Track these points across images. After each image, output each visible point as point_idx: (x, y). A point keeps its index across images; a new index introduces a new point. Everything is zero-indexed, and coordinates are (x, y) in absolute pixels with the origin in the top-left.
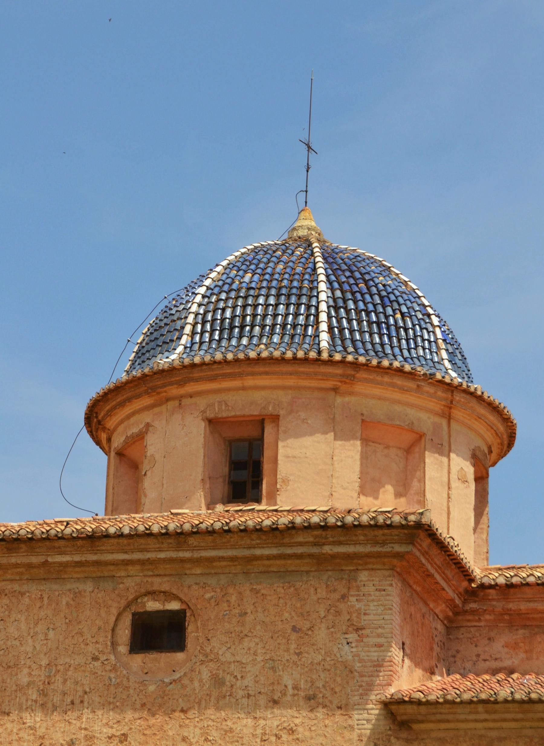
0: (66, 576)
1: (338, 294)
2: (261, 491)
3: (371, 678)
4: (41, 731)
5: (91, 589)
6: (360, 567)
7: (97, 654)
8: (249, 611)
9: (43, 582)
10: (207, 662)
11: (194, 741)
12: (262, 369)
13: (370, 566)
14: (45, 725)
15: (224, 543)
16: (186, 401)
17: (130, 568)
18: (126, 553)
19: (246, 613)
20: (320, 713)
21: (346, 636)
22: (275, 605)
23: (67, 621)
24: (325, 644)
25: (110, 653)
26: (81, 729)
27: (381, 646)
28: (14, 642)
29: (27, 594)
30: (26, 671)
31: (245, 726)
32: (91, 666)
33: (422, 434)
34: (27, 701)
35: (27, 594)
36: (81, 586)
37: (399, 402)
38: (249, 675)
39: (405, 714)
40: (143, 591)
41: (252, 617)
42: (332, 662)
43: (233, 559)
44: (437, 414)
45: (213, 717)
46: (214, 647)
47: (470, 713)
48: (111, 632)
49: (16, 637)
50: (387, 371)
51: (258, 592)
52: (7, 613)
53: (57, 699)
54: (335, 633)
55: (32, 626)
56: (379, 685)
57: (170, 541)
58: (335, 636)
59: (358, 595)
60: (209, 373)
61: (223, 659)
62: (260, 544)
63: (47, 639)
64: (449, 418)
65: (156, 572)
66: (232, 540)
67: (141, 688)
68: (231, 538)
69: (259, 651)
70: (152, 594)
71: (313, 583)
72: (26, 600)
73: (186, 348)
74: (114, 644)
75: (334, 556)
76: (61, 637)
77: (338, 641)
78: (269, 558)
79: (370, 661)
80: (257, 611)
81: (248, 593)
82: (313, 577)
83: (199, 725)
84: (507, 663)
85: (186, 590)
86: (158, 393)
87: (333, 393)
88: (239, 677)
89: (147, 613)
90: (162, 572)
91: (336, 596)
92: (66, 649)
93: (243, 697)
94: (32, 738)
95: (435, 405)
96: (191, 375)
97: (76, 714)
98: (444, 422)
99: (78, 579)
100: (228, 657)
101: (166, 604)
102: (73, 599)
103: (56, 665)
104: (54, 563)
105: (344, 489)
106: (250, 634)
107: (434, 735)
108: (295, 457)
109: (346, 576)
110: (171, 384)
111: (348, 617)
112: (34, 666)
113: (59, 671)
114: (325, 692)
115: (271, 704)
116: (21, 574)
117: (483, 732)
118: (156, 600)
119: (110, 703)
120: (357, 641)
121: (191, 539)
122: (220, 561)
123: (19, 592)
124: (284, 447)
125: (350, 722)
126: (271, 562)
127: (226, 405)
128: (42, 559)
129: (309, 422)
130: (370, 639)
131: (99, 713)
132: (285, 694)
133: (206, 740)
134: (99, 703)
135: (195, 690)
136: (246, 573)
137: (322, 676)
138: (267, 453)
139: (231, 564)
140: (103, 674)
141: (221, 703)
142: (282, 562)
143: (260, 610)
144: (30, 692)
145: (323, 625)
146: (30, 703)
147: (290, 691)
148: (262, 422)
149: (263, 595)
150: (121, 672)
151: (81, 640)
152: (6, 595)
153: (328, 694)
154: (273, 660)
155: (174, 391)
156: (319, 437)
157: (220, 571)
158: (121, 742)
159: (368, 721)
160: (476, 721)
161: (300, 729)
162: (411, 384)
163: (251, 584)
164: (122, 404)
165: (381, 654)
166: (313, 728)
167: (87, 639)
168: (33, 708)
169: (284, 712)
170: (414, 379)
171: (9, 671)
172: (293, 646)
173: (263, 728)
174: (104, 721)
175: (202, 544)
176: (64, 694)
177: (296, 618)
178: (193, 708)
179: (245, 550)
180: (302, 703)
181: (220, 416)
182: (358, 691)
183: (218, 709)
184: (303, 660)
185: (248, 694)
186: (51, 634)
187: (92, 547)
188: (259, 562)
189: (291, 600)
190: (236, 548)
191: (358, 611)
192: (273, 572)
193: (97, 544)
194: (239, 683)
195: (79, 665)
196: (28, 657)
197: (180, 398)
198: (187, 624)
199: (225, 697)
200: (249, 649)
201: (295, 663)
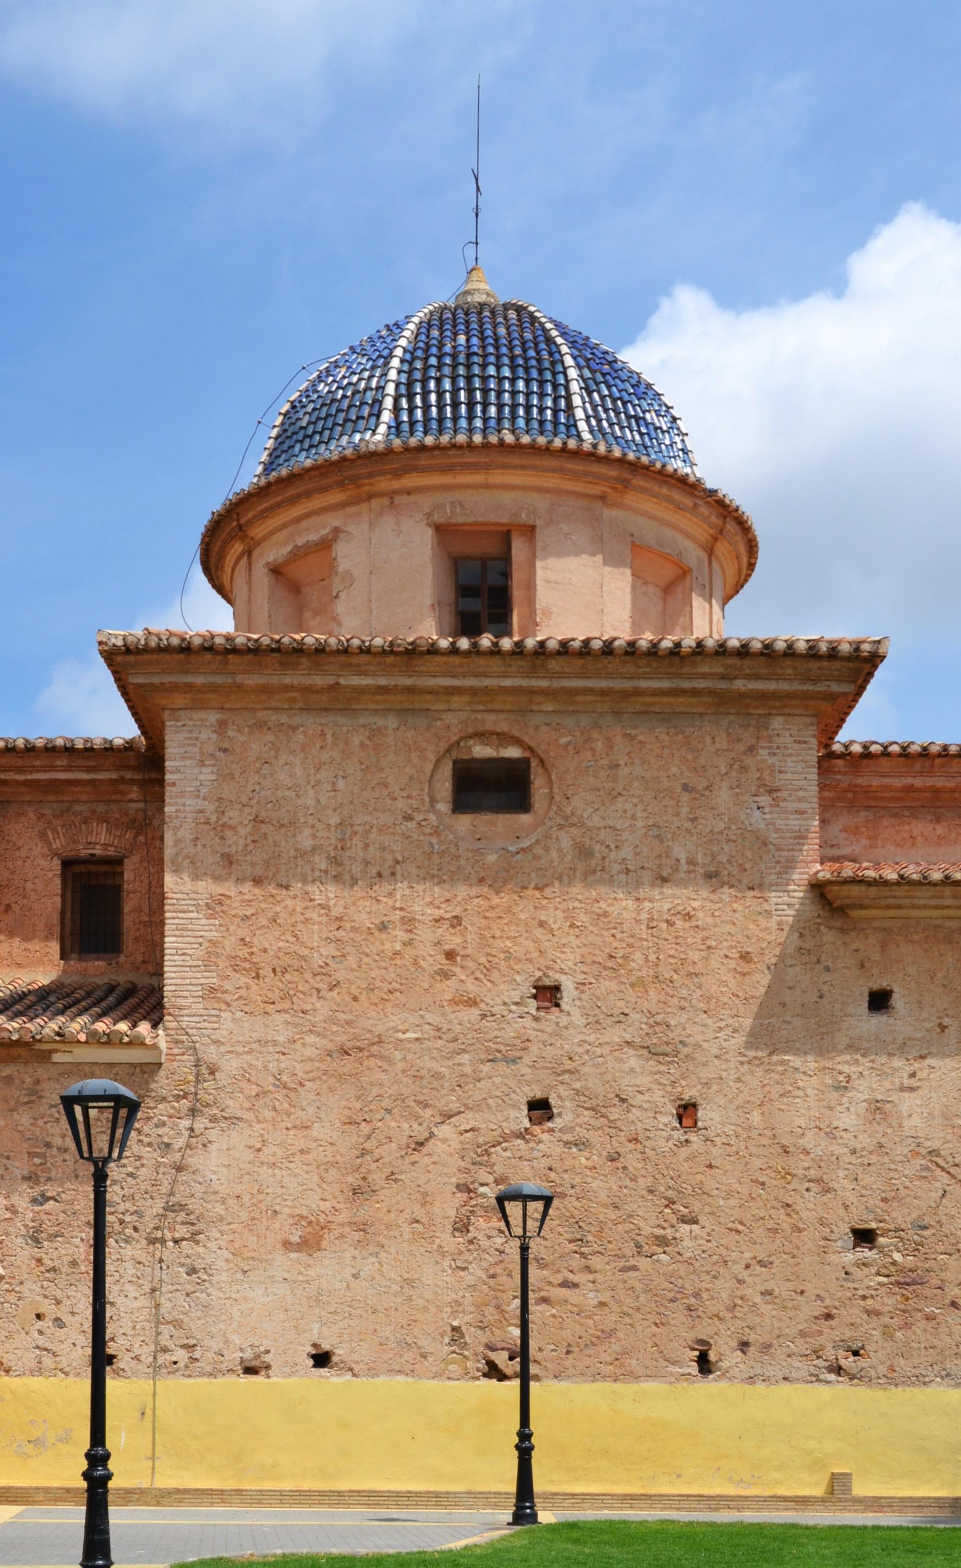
0: (358, 707)
2: (511, 625)
3: (791, 853)
4: (337, 911)
5: (395, 725)
6: (774, 712)
7: (409, 812)
8: (622, 762)
9: (324, 714)
10: (568, 826)
11: (555, 926)
12: (518, 461)
13: (787, 711)
14: (342, 902)
15: (599, 669)
16: (401, 500)
17: (455, 698)
18: (455, 677)
19: (618, 766)
20: (726, 893)
21: (757, 799)
22: (657, 756)
23: (363, 767)
24: (729, 809)
25: (429, 812)
26: (395, 908)
27: (803, 812)
28: (287, 793)
29: (302, 729)
30: (307, 832)
31: (625, 909)
32: (403, 827)
33: (686, 568)
34: (313, 870)
35: (302, 729)
36: (380, 722)
37: (668, 524)
38: (626, 845)
39: (848, 897)
40: (470, 730)
41: (627, 771)
42: (739, 831)
43: (603, 693)
45: (579, 897)
46: (576, 808)
47: (934, 897)
48: (427, 784)
49: (289, 785)
50: (669, 479)
51: (633, 738)
52: (272, 753)
53: (356, 869)
54: (742, 794)
55: (312, 772)
56: (802, 861)
57: (521, 663)
58: (741, 798)
59: (770, 748)
60: (442, 461)
61: (589, 823)
62: (647, 673)
63: (335, 791)
64: (710, 552)
65: (490, 706)
66: (610, 666)
67: (476, 858)
68: (610, 662)
69: (639, 815)
70: (480, 735)
71: (709, 729)
72: (300, 737)
73: (389, 427)
74: (433, 801)
75: (743, 695)
76: (355, 787)
77: (745, 805)
78: (654, 693)
79: (791, 831)
80: (633, 763)
81: (619, 739)
82: (709, 721)
83: (562, 906)
85: (531, 732)
86: (360, 486)
87: (600, 503)
88: (613, 846)
89: (474, 760)
90: (497, 706)
91: (741, 747)
92: (364, 804)
93: (620, 873)
94: (325, 919)
95: (702, 532)
96: (416, 462)
97: (386, 888)
98: (705, 557)
99: (376, 711)
100: (596, 820)
101: (501, 749)
102: (369, 737)
103: (352, 825)
104: (347, 686)
105: (615, 629)
106: (625, 793)
107: (877, 924)
108: (557, 583)
109: (754, 722)
110: (382, 473)
111: (758, 775)
112: (319, 826)
113: (356, 833)
114: (731, 869)
115: (658, 882)
116: (294, 700)
117: (940, 922)
118: (487, 745)
119: (433, 876)
120: (771, 805)
121: (552, 661)
122: (585, 695)
123: (289, 726)
124: (543, 568)
125: (766, 906)
126: (657, 699)
127: (462, 506)
128: (331, 680)
129: (573, 537)
130: (789, 804)
131: (420, 888)
132: (677, 870)
133: (572, 925)
134: (418, 876)
135: (552, 862)
136: (617, 713)
137: (726, 848)
138: (518, 576)
139: (599, 699)
140: (421, 838)
141: (590, 879)
142: (672, 699)
143: (637, 761)
144: (316, 859)
145: (725, 784)
146: (317, 874)
147: (684, 866)
148: (509, 532)
149: (640, 742)
150: (447, 836)
151: (385, 792)
152: (269, 729)
153: (735, 871)
154: (658, 827)
155: (384, 484)
156: (585, 559)
157: (580, 708)
158: (453, 927)
159: (789, 905)
160: (936, 907)
161: (700, 914)
162: (688, 501)
163: (623, 727)
164: (293, 501)
165: (804, 823)
166: (717, 914)
167: (394, 792)
168: (323, 880)
169: (677, 892)
170: (692, 495)
171: (283, 830)
172: (685, 810)
173: (649, 912)
174: (427, 900)
175: (567, 670)
176: (367, 863)
177: (687, 773)
178: (552, 884)
179: (625, 681)
180: (700, 881)
181: (454, 521)
182: (775, 868)
183: (588, 885)
184: (700, 827)
185: (627, 869)
186: (341, 784)
187: (407, 666)
188: (640, 699)
189: (679, 750)
190: (612, 678)
191: (772, 769)
192: (655, 712)
193: (415, 662)
194: (613, 855)
195: (385, 825)
196: (309, 813)
197: (392, 494)
198: (532, 777)
199: (594, 872)
200: (625, 811)
201: (688, 831)
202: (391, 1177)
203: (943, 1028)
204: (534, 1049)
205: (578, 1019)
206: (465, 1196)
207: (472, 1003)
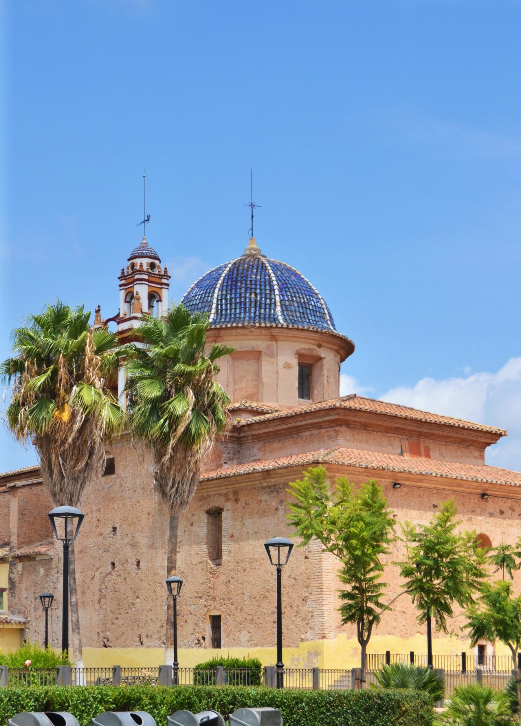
1: (224, 292)
44: (268, 340)
84: (258, 457)
161: (141, 501)
202: (88, 588)
203: (185, 531)
204: (112, 546)
205: (119, 538)
206: (100, 593)
207: (101, 534)
